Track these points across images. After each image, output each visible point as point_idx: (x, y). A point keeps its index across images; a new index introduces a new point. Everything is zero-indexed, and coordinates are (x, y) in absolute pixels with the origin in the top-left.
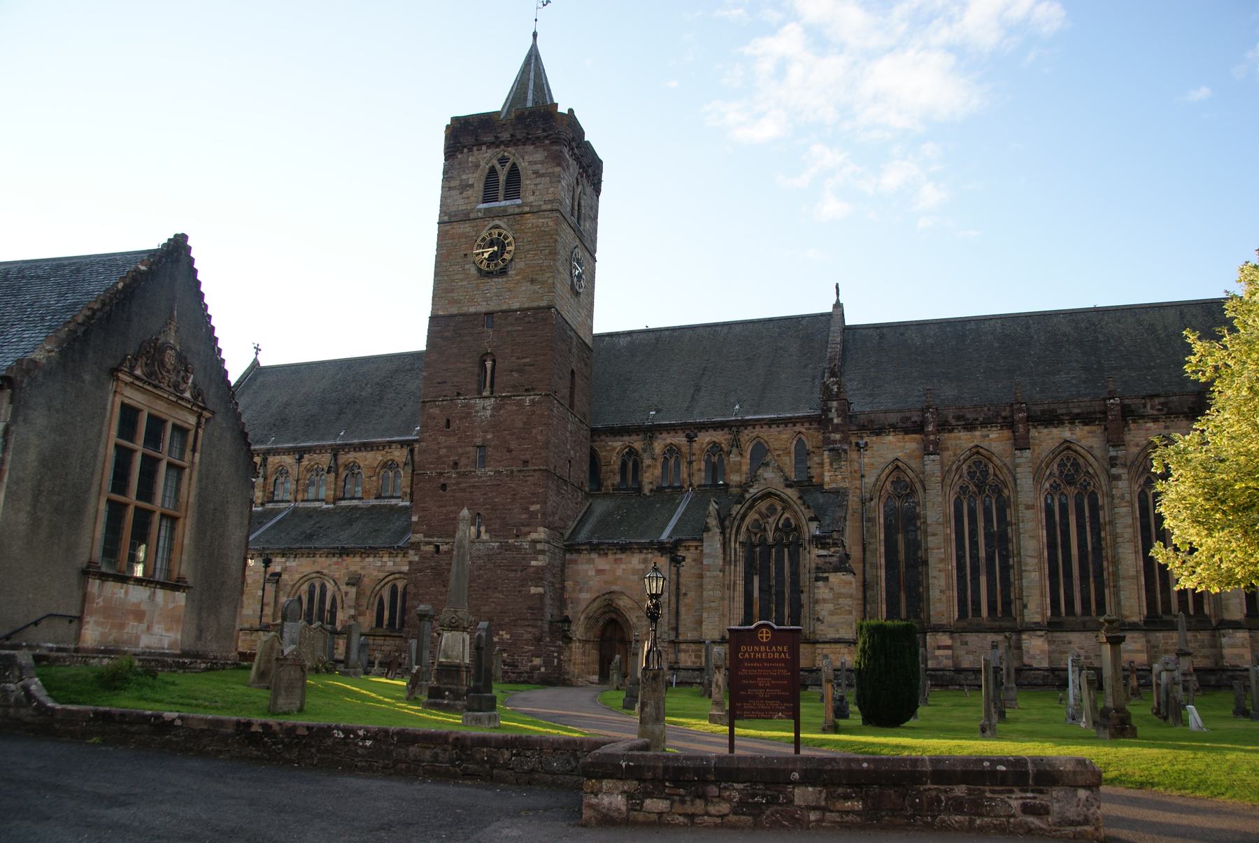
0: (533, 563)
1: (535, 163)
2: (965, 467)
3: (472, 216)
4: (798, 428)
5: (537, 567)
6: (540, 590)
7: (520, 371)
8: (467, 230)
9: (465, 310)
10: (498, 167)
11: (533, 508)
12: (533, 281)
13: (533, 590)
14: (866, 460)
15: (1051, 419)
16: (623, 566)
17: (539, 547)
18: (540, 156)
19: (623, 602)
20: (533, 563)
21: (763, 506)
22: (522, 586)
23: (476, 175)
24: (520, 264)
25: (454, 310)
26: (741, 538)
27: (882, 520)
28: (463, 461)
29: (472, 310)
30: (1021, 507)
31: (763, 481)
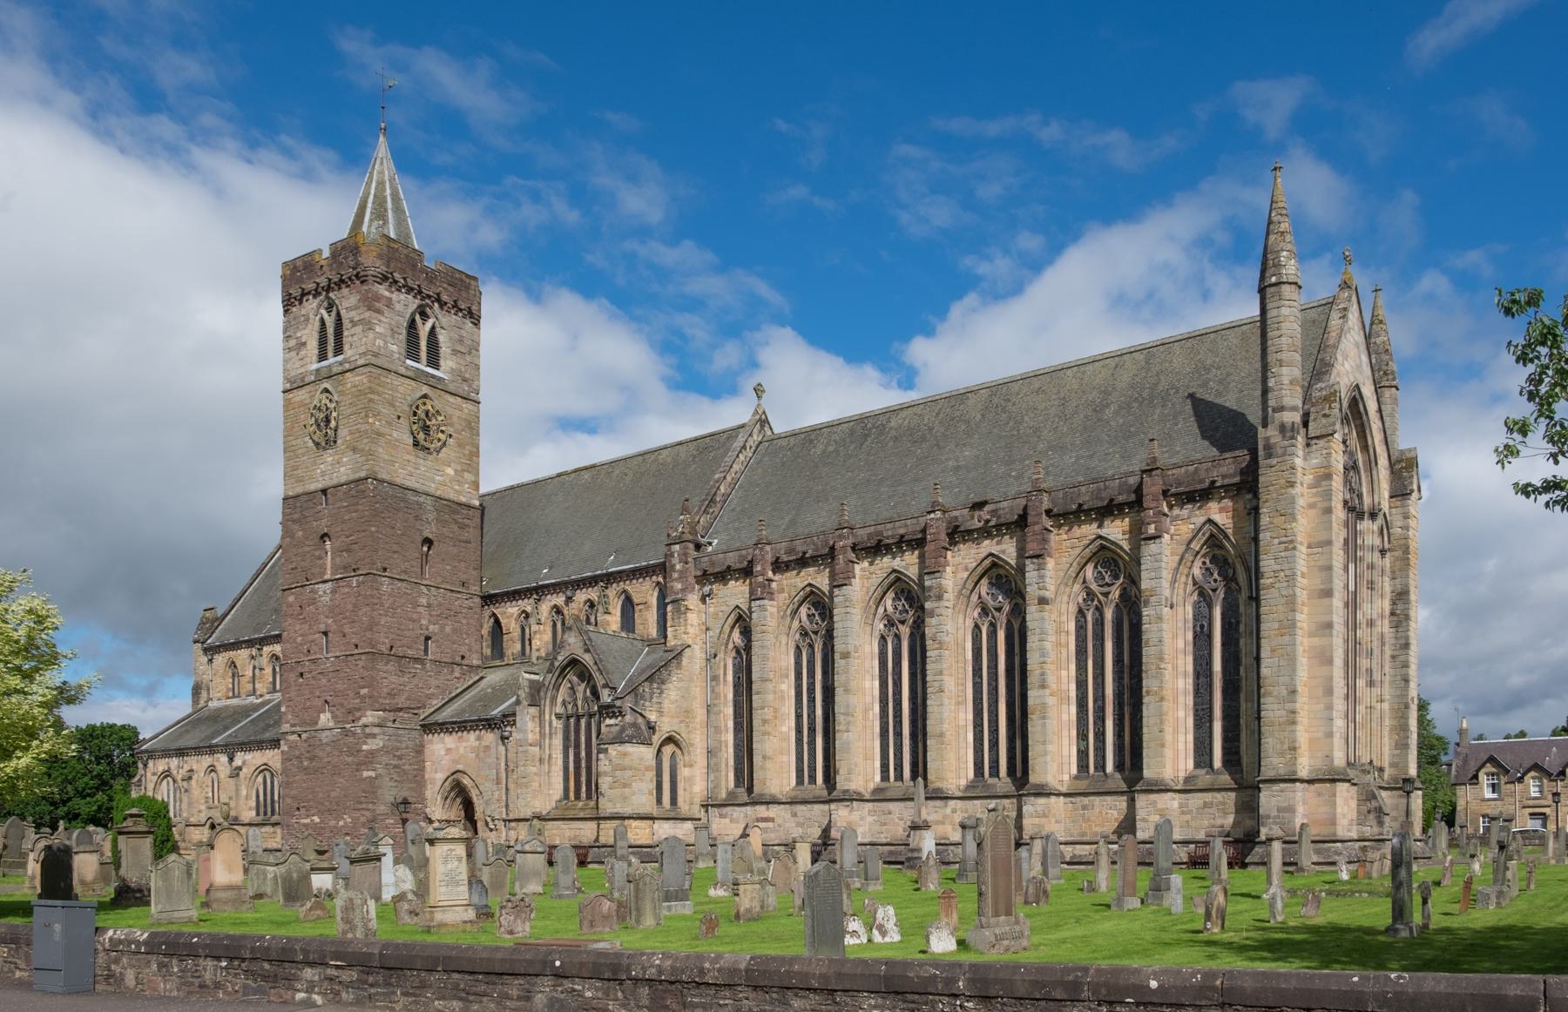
0: (365, 747)
2: (803, 611)
5: (367, 751)
6: (372, 774)
8: (304, 397)
13: (366, 774)
14: (712, 610)
15: (875, 549)
16: (464, 744)
17: (368, 730)
19: (466, 781)
20: (365, 747)
22: (357, 770)
27: (730, 678)
28: (314, 648)
30: (837, 656)
31: (568, 647)
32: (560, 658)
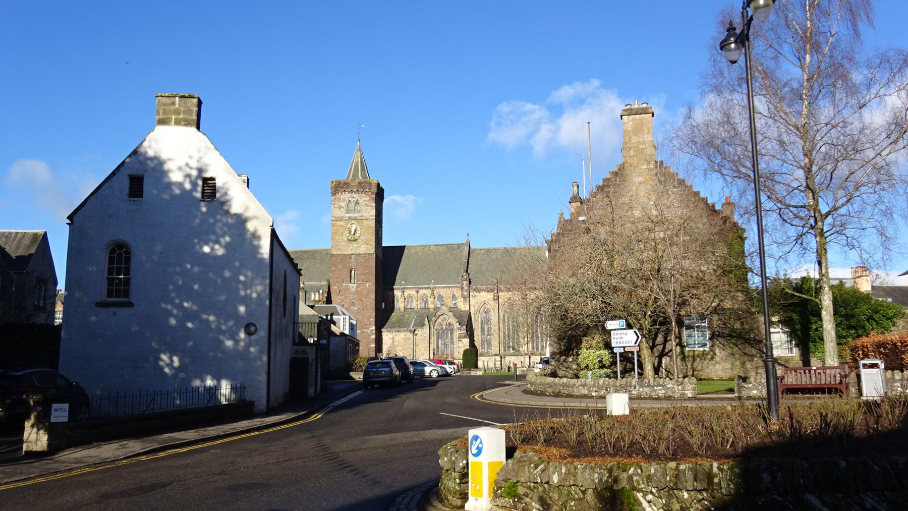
1: (366, 201)
3: (344, 219)
4: (453, 289)
7: (365, 274)
9: (344, 253)
10: (352, 201)
11: (371, 320)
12: (367, 244)
18: (367, 198)
21: (442, 317)
23: (344, 203)
24: (362, 238)
25: (340, 253)
26: (435, 327)
29: (346, 253)
32: (439, 313)
